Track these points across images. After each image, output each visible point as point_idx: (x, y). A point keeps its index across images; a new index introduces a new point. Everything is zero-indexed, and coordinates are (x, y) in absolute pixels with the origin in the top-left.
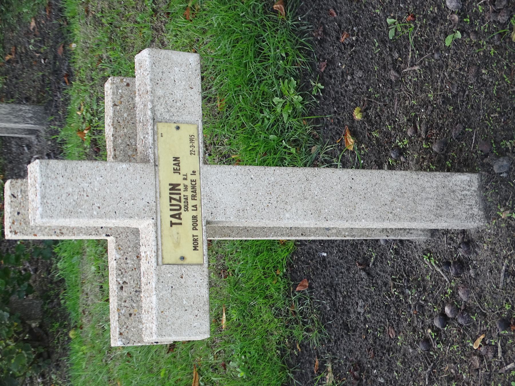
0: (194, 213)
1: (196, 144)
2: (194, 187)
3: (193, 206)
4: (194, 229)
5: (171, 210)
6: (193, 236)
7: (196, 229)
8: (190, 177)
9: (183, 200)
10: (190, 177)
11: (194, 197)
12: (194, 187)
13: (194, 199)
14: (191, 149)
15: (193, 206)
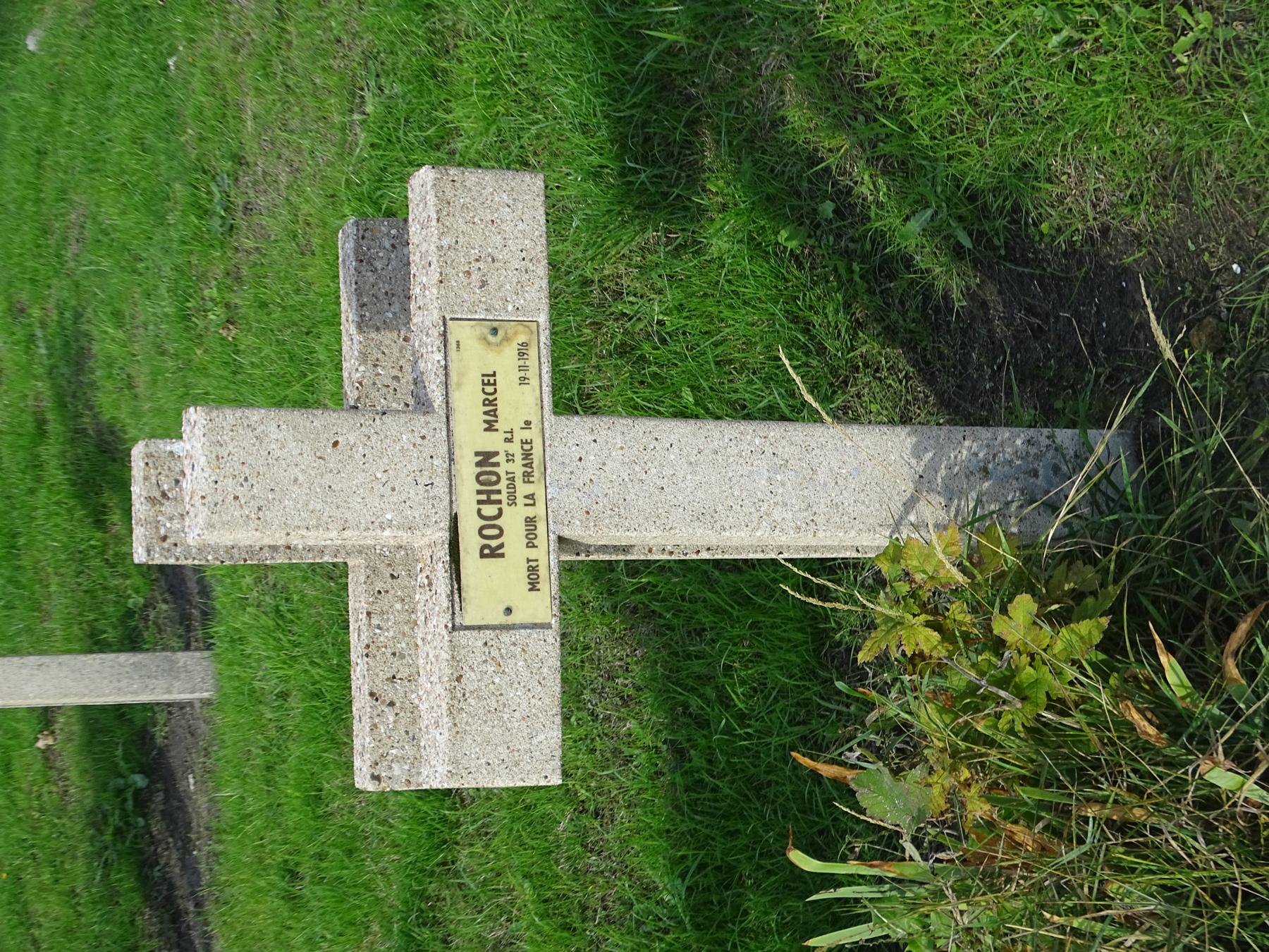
0: (530, 512)
1: (532, 362)
2: (527, 455)
3: (526, 497)
4: (531, 545)
5: (479, 492)
6: (529, 561)
7: (534, 546)
8: (519, 435)
9: (502, 485)
10: (519, 435)
11: (527, 477)
12: (527, 455)
13: (529, 482)
14: (522, 374)
15: (526, 497)
